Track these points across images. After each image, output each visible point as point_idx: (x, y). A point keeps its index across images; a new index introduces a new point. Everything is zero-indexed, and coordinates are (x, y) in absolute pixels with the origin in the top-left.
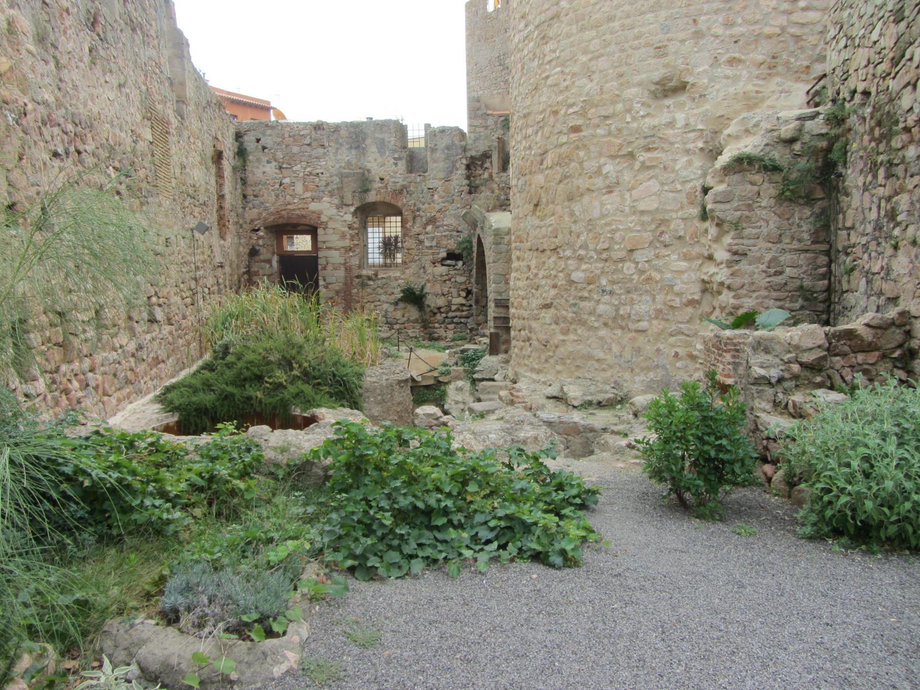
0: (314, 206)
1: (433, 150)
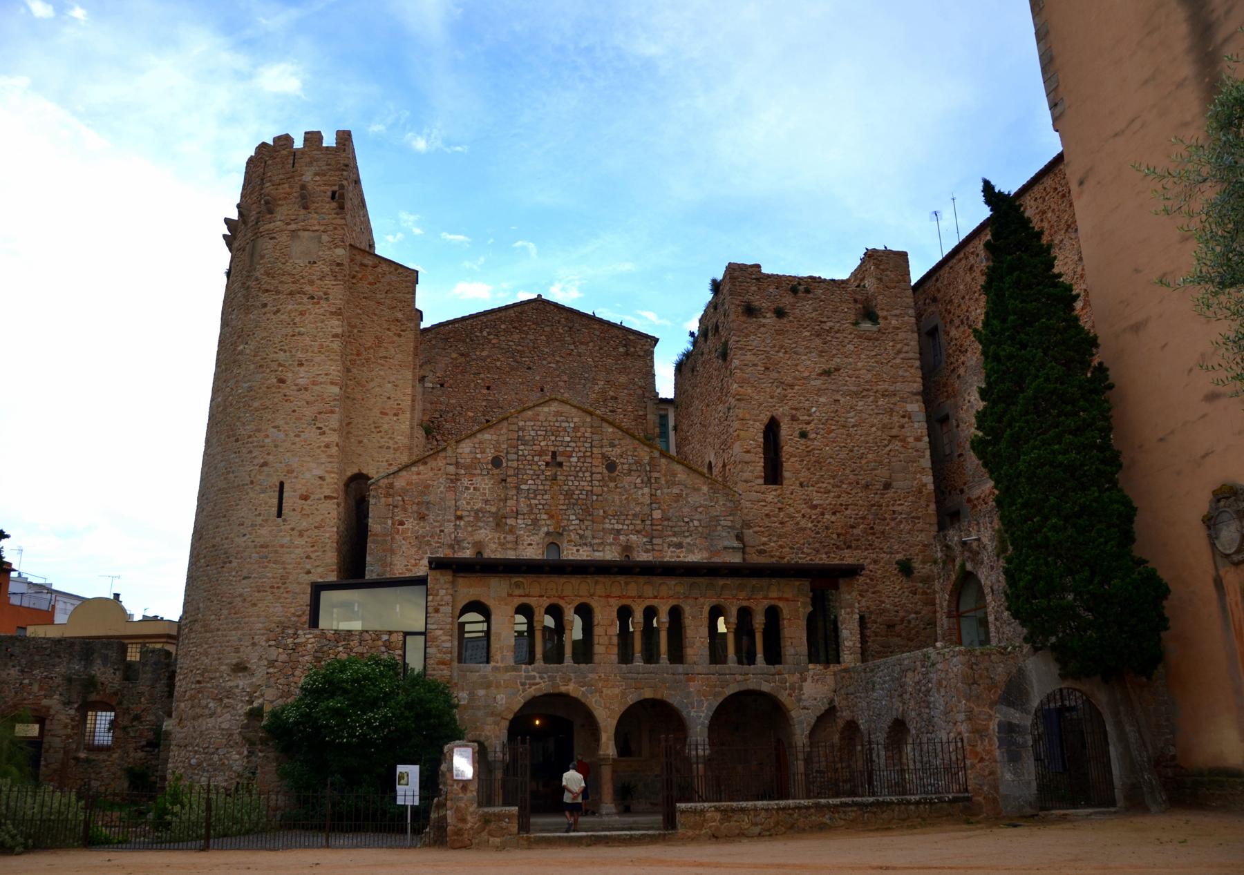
0: (45, 702)
1: (145, 665)
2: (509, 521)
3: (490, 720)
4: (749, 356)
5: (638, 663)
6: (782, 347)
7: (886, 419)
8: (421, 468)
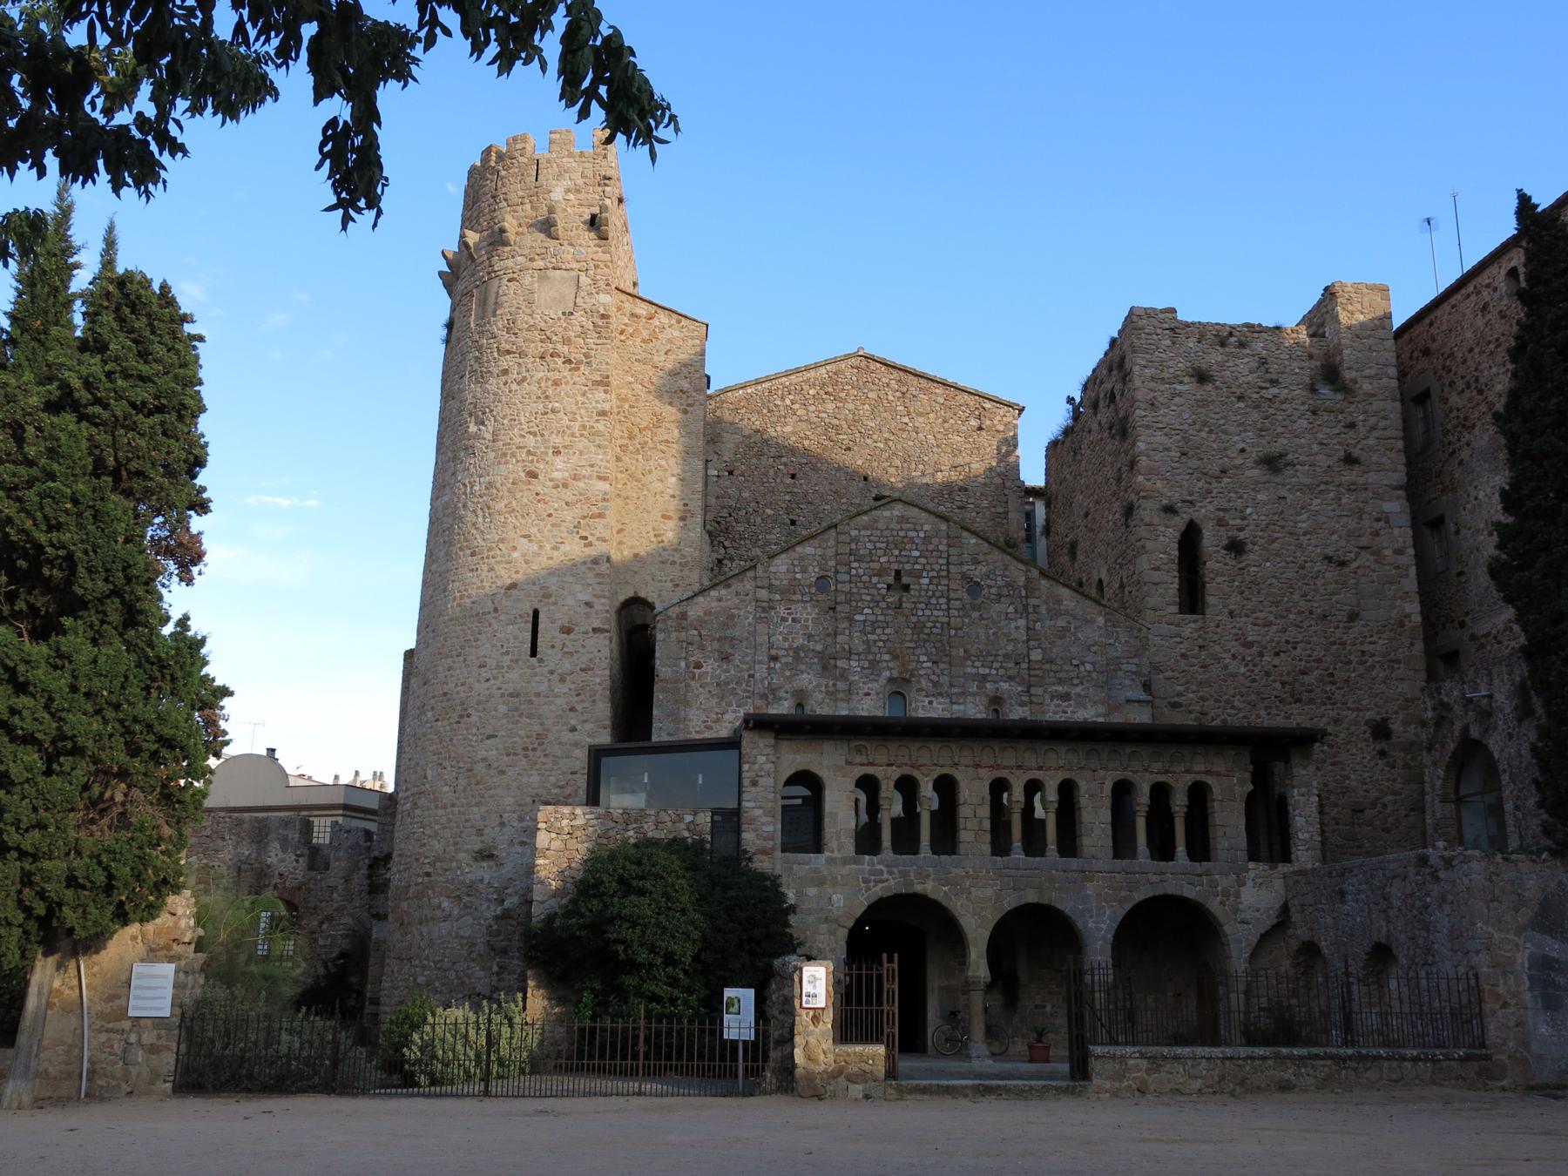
1: (338, 848)
2: (839, 664)
3: (824, 927)
4: (1159, 438)
5: (1018, 854)
6: (1205, 424)
7: (1352, 524)
8: (723, 592)
